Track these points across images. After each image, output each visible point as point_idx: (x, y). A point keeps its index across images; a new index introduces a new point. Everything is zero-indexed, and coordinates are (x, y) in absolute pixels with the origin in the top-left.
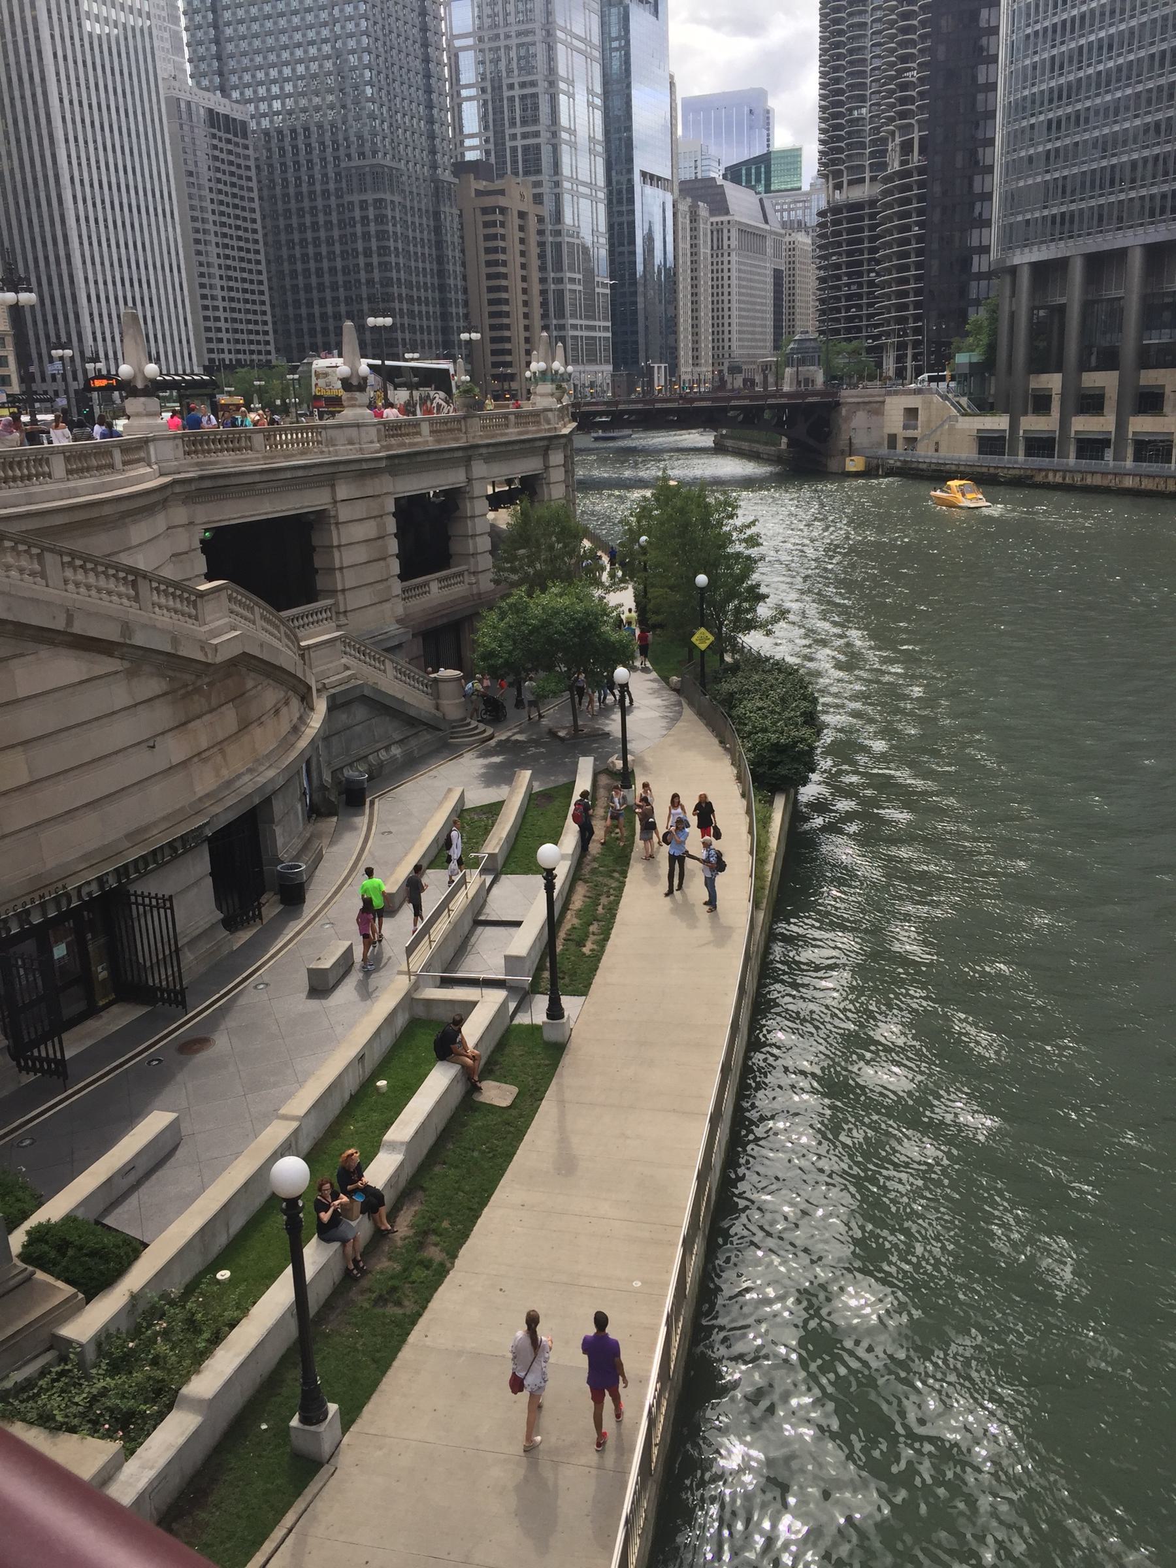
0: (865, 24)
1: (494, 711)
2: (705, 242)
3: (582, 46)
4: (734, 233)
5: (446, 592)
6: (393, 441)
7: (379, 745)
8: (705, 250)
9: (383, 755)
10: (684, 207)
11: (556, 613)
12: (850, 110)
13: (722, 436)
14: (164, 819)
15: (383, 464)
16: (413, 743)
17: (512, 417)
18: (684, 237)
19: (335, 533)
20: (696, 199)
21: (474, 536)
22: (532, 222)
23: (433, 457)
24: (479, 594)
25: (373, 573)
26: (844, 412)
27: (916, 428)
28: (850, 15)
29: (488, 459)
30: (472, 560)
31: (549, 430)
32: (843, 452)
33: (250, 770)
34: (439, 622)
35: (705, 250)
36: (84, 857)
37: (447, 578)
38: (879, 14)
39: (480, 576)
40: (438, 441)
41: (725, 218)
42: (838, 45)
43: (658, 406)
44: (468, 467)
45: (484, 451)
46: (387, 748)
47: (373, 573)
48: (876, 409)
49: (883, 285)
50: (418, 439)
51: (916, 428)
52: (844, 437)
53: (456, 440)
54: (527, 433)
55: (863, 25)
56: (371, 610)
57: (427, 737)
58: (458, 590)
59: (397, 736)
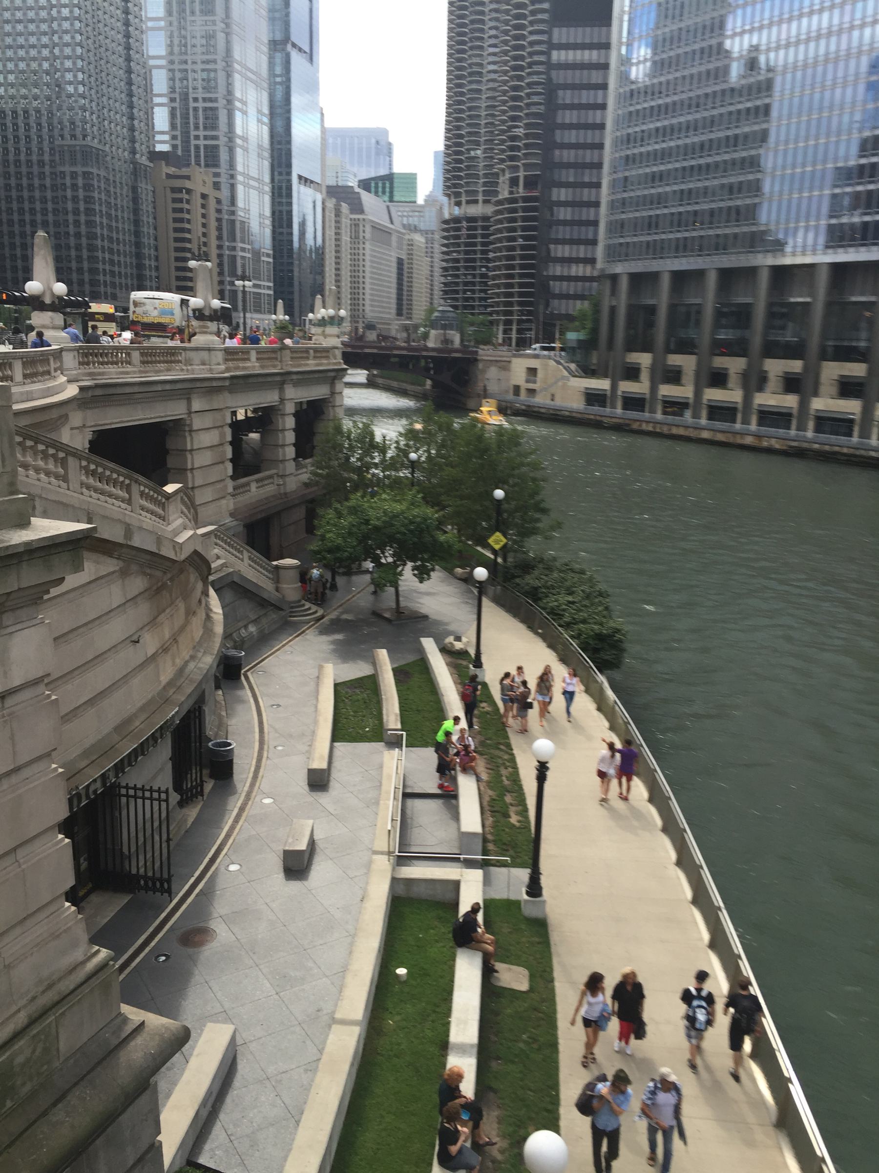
0: (481, 90)
1: (319, 594)
4: (368, 229)
5: (262, 491)
6: (230, 364)
7: (241, 624)
8: (346, 238)
9: (243, 632)
10: (331, 204)
11: (396, 516)
12: (468, 150)
13: (374, 375)
14: (142, 709)
15: (227, 383)
16: (264, 621)
17: (311, 352)
19: (188, 439)
20: (339, 199)
21: (283, 446)
23: (261, 380)
24: (285, 494)
25: (215, 474)
28: (470, 82)
29: (296, 384)
30: (281, 465)
31: (335, 364)
32: (479, 396)
33: (193, 657)
34: (259, 516)
35: (346, 238)
36: (86, 753)
37: (261, 480)
38: (491, 85)
39: (287, 479)
40: (262, 367)
41: (361, 217)
42: (460, 103)
43: (367, 351)
44: (281, 390)
45: (294, 377)
46: (246, 627)
47: (215, 474)
49: (494, 278)
50: (248, 364)
52: (481, 384)
53: (274, 366)
54: (321, 365)
55: (479, 91)
56: (212, 506)
57: (274, 616)
58: (270, 489)
59: (253, 617)
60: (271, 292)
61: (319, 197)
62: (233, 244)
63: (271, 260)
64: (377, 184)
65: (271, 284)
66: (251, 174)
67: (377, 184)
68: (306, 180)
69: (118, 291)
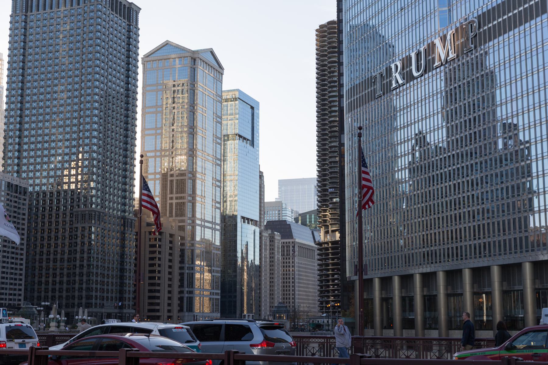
2: (278, 252)
8: (278, 256)
18: (266, 249)
35: (278, 256)
41: (291, 240)
60: (219, 297)
61: (258, 230)
64: (310, 216)
65: (219, 292)
66: (206, 219)
67: (310, 216)
68: (248, 219)
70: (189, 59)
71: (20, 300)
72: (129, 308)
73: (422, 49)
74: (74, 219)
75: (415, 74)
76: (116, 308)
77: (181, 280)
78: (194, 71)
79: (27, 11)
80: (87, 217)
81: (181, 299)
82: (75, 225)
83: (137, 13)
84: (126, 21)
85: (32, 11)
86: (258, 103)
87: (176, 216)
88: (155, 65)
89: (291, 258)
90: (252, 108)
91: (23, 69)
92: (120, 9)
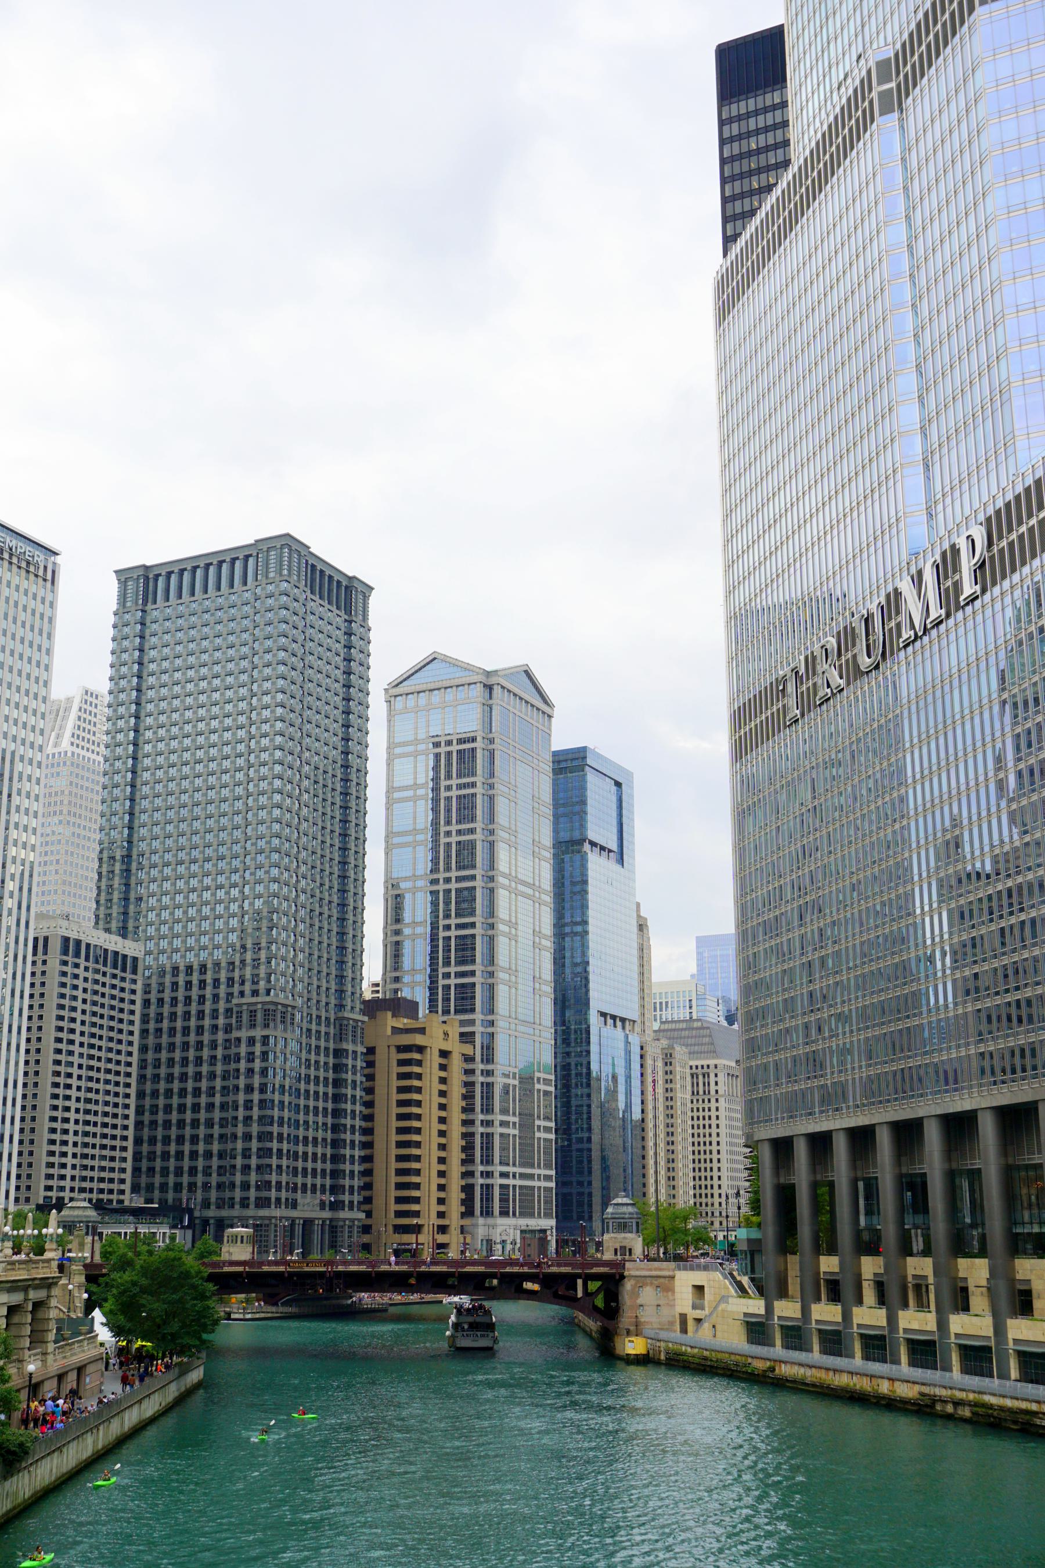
3: (530, 892)
8: (683, 1095)
22: (456, 1064)
26: (628, 1285)
27: (703, 1309)
35: (683, 1095)
48: (666, 1285)
51: (703, 1309)
60: (553, 1185)
62: (489, 1117)
63: (553, 1136)
65: (553, 1173)
68: (614, 1017)
69: (299, 1195)
70: (479, 687)
71: (122, 1192)
72: (351, 1208)
73: (873, 607)
74: (234, 1021)
75: (865, 662)
76: (322, 1206)
77: (468, 1149)
78: (489, 708)
79: (145, 602)
80: (259, 1016)
81: (468, 1190)
82: (235, 1034)
83: (366, 598)
84: (342, 613)
85: (155, 602)
86: (630, 775)
87: (456, 1012)
88: (411, 700)
89: (713, 1100)
90: (618, 784)
91: (137, 717)
92: (330, 591)
